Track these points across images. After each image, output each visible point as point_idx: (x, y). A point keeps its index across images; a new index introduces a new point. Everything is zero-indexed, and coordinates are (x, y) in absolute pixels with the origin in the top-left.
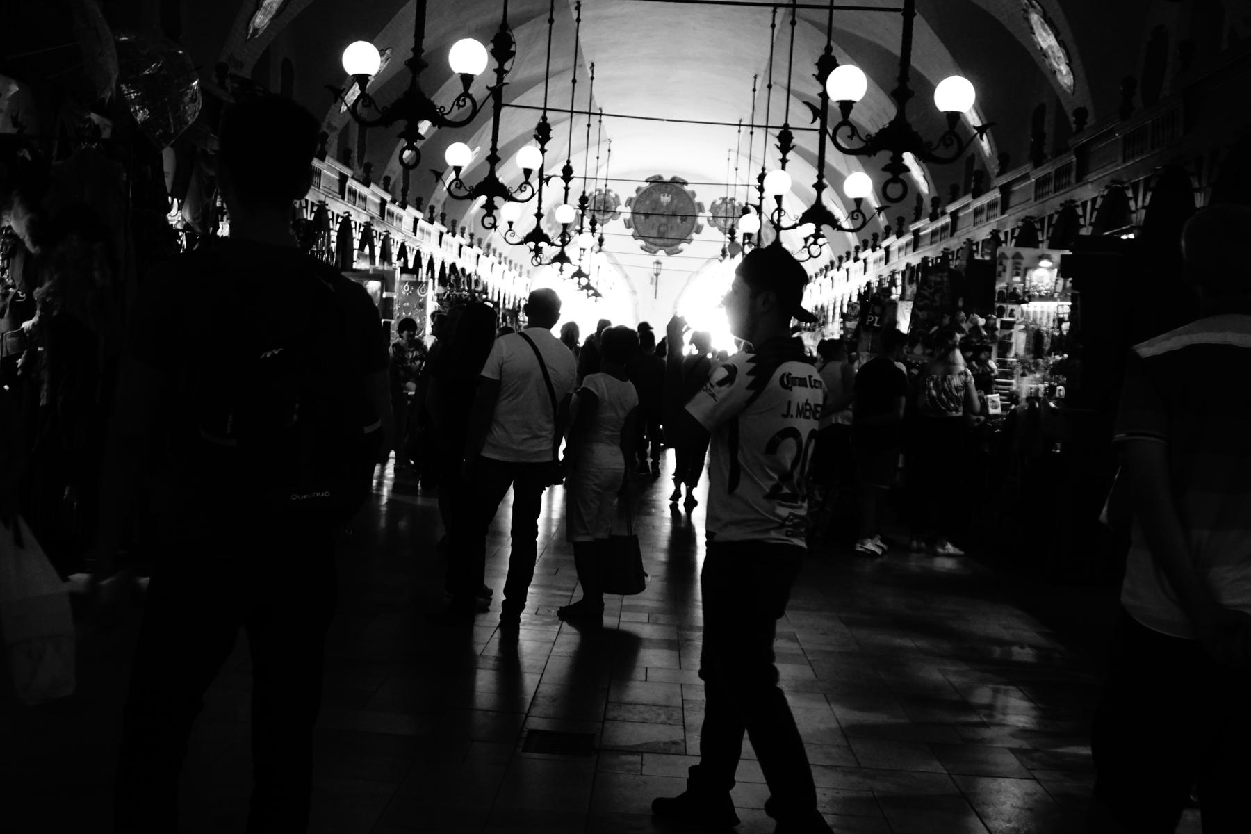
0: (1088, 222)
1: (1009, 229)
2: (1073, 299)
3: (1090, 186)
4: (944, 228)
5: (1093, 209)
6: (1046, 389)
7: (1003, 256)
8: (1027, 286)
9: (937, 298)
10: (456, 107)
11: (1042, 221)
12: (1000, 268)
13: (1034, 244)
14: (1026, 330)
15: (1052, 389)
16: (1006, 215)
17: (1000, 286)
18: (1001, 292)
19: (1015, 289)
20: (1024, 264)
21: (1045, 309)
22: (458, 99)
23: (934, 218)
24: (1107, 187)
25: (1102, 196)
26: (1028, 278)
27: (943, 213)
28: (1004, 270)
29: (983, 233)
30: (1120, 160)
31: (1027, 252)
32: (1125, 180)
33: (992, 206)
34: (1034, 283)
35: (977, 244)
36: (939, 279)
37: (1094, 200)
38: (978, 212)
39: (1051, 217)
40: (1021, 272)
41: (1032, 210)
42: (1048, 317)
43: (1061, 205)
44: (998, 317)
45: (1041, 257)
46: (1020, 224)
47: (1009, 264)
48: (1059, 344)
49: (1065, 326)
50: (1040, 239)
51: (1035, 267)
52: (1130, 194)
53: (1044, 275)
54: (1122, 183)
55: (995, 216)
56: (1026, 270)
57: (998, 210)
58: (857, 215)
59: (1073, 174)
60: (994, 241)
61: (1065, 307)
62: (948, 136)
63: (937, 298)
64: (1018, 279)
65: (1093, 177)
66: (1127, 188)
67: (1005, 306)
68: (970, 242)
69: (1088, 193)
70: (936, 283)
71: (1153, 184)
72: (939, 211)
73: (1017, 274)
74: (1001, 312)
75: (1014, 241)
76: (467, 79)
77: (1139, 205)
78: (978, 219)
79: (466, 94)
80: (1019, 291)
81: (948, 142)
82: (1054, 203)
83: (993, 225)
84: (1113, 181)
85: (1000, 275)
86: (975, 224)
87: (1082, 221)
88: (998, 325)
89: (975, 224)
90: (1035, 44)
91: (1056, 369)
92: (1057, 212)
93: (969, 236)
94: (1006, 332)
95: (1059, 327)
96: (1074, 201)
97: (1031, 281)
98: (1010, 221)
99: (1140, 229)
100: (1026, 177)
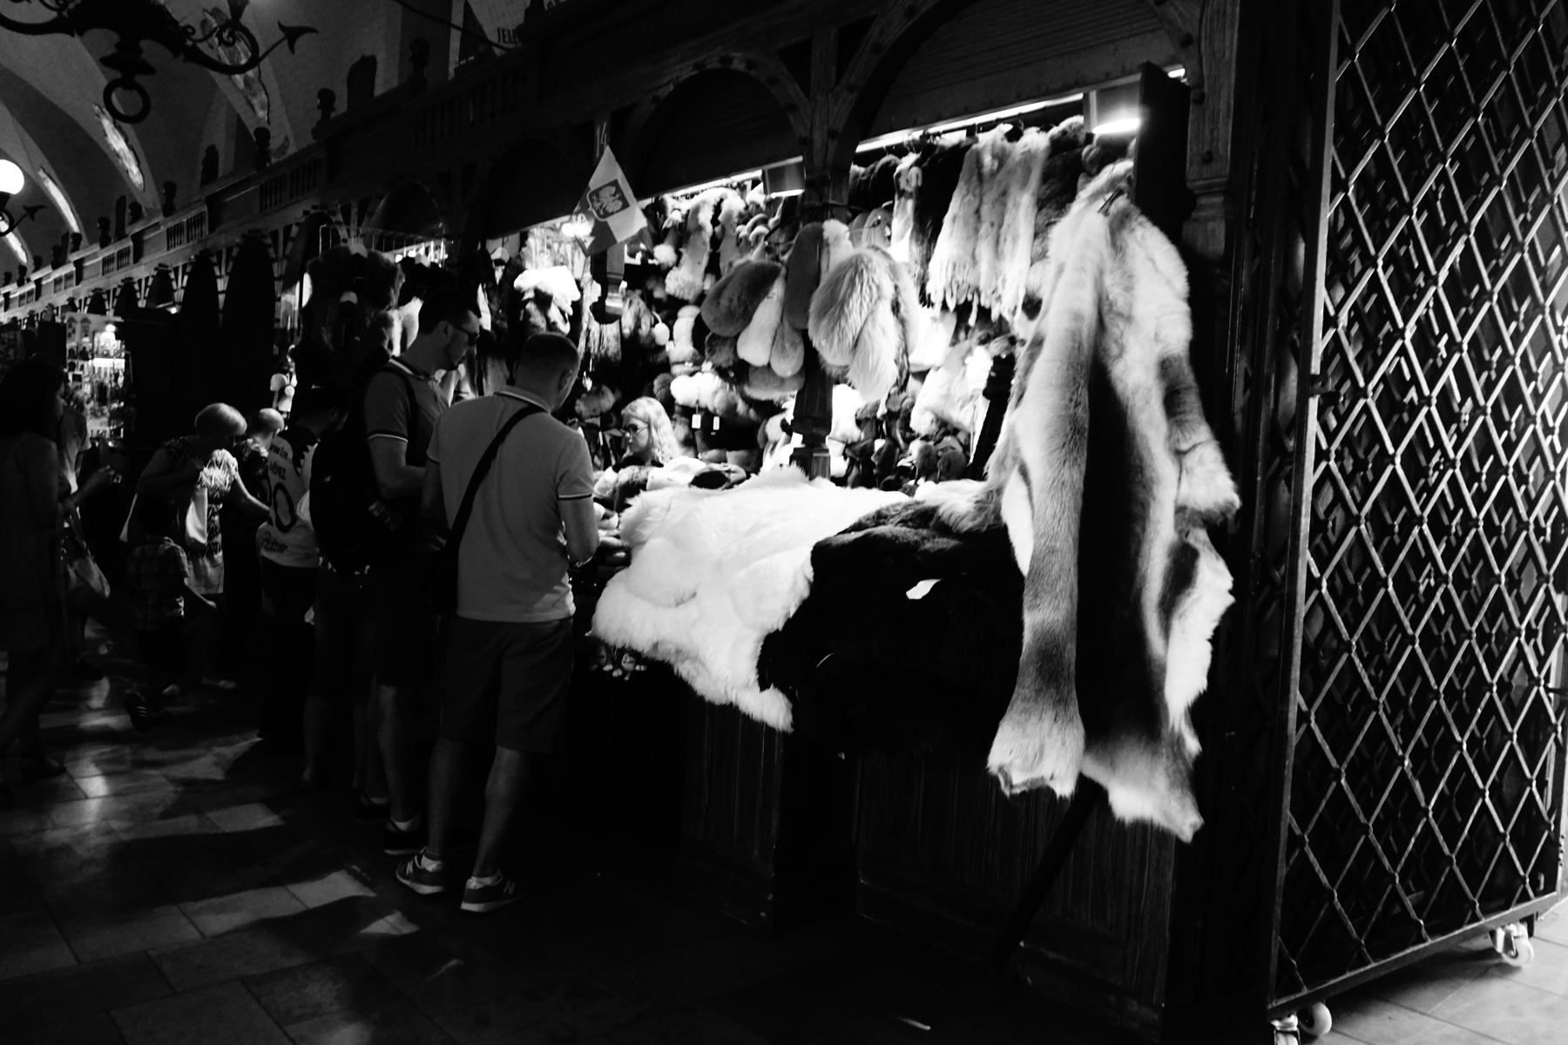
1: (82, 297)
2: (126, 357)
3: (143, 267)
4: (30, 293)
5: (146, 286)
6: (111, 431)
7: (72, 320)
8: (96, 345)
9: (11, 352)
11: (108, 292)
12: (69, 330)
13: (103, 312)
14: (90, 382)
15: (117, 432)
16: (80, 286)
17: (70, 345)
18: (71, 350)
19: (84, 348)
20: (92, 327)
21: (103, 367)
23: (21, 284)
24: (156, 269)
26: (96, 339)
27: (29, 280)
28: (74, 331)
29: (61, 300)
30: (166, 248)
31: (94, 318)
32: (169, 264)
33: (68, 277)
34: (102, 344)
35: (57, 308)
36: (12, 337)
37: (147, 279)
38: (57, 281)
39: (115, 290)
40: (90, 334)
41: (100, 282)
42: (105, 374)
43: (122, 281)
44: (70, 370)
45: (107, 323)
46: (91, 294)
47: (78, 327)
48: (117, 394)
49: (121, 380)
51: (103, 330)
53: (108, 338)
54: (167, 267)
55: (71, 286)
56: (94, 333)
57: (74, 281)
59: (131, 255)
60: (71, 306)
61: (120, 364)
63: (11, 352)
64: (86, 340)
65: (143, 260)
67: (76, 362)
68: (51, 306)
69: (142, 272)
70: (9, 340)
71: (188, 269)
73: (86, 336)
74: (72, 367)
75: (86, 308)
77: (180, 284)
78: (58, 287)
80: (88, 350)
82: (115, 280)
83: (69, 293)
84: (160, 265)
85: (70, 336)
86: (55, 292)
88: (70, 378)
89: (55, 292)
90: (109, 146)
91: (114, 416)
92: (119, 286)
93: (50, 301)
94: (79, 384)
95: (116, 380)
96: (131, 279)
97: (99, 342)
98: (83, 291)
99: (184, 305)
100: (95, 256)
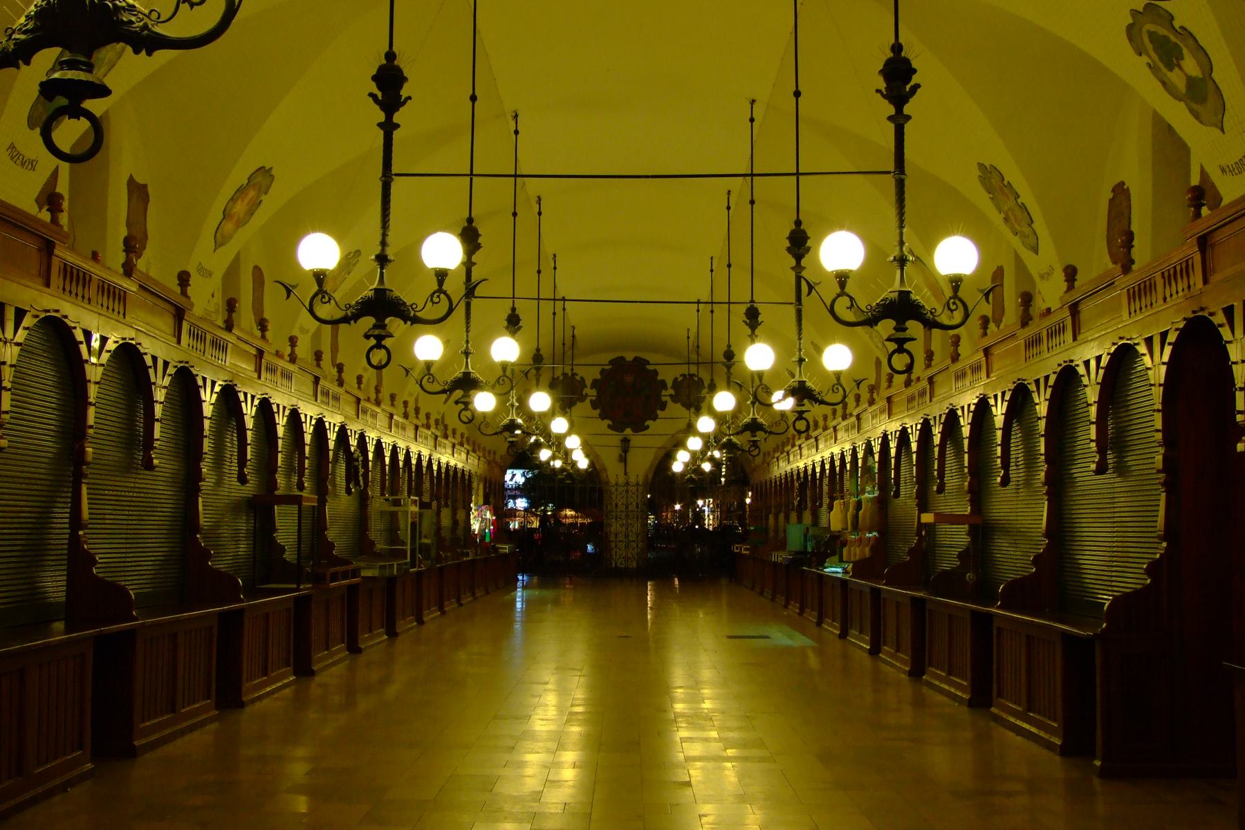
0: (1093, 381)
4: (922, 394)
10: (429, 304)
11: (1037, 382)
22: (432, 295)
25: (1108, 354)
50: (1037, 401)
52: (1142, 349)
58: (837, 389)
62: (952, 301)
66: (1137, 344)
72: (914, 377)
76: (441, 275)
78: (960, 384)
79: (440, 290)
81: (953, 307)
87: (1085, 381)
